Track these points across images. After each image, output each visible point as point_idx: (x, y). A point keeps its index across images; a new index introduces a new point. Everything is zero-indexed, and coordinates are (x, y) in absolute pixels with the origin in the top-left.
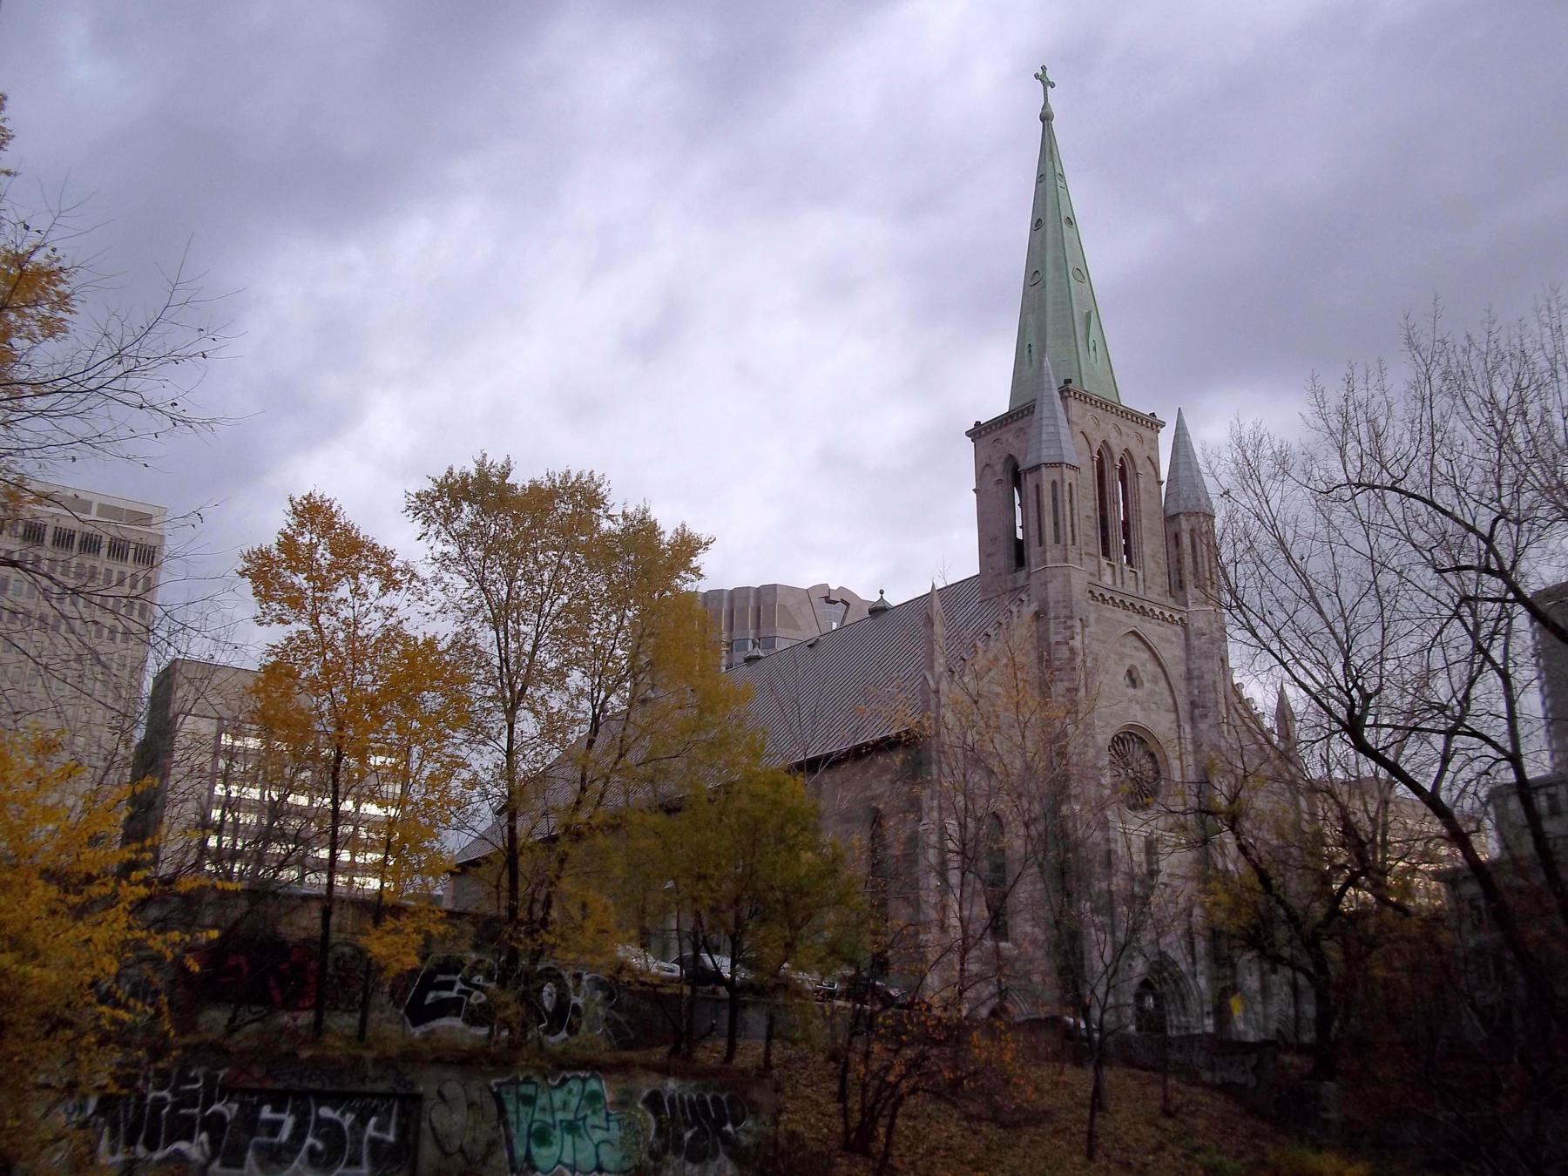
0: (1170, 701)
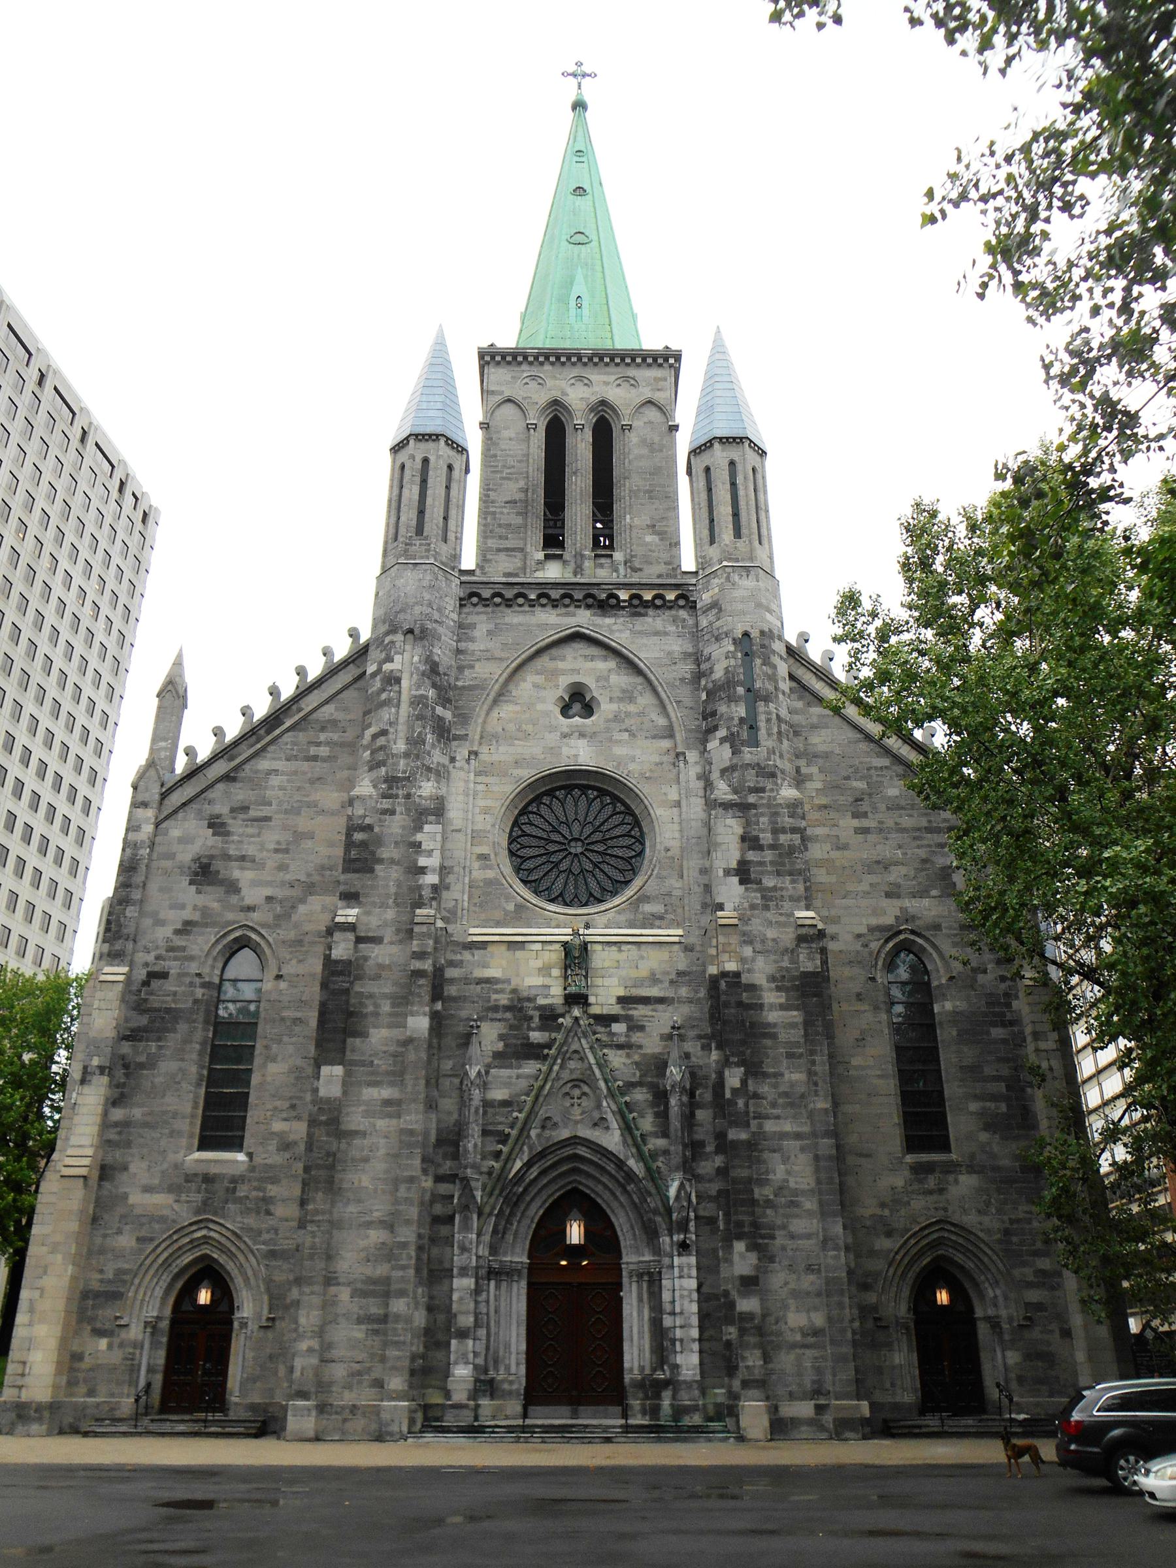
0: (662, 721)
